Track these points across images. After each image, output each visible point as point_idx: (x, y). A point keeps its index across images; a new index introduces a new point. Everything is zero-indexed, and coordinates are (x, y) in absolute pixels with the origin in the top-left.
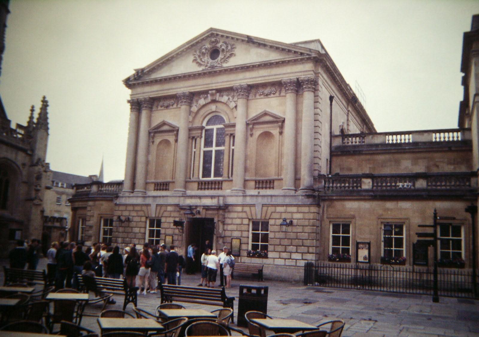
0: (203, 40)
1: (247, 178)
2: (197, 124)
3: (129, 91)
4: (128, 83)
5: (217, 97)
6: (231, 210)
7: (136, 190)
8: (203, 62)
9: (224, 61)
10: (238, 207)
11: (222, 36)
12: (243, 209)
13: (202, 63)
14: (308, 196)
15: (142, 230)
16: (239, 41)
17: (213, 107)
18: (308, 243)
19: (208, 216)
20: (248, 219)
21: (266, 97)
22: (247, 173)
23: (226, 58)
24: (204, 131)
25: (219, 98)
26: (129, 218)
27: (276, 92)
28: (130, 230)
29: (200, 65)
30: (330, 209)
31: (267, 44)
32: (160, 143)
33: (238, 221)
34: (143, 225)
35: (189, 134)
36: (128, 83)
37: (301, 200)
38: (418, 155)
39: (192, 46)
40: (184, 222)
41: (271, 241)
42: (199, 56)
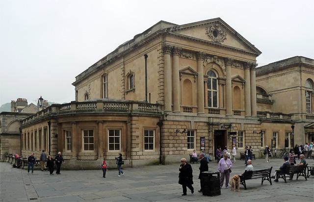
14: (259, 120)
17: (214, 66)
38: (259, 104)
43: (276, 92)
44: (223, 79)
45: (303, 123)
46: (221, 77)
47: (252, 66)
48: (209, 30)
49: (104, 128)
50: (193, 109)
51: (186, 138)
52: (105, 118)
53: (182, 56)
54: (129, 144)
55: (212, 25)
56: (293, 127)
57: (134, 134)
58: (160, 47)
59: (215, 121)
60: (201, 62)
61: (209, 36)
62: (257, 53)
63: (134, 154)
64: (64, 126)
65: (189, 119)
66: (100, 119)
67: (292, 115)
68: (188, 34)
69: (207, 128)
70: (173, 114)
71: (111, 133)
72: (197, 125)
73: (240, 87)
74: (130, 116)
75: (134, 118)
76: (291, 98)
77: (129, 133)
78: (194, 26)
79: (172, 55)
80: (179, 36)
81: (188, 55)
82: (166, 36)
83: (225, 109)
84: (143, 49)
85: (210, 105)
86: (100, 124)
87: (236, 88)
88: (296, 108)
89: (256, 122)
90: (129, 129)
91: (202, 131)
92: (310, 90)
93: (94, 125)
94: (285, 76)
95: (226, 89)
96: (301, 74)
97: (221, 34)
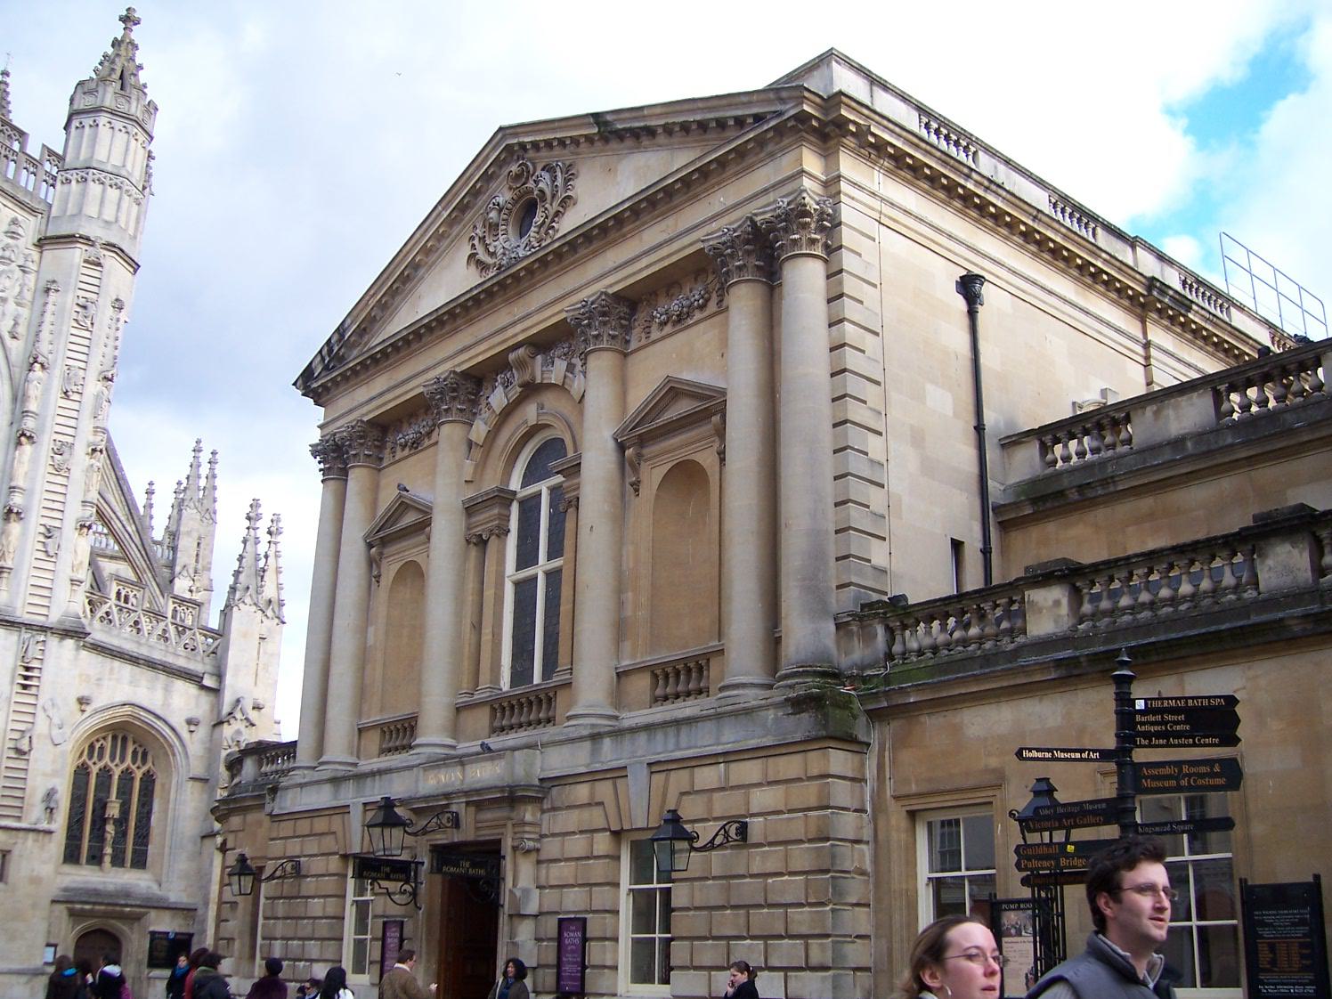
0: (487, 177)
1: (626, 663)
2: (490, 483)
3: (319, 414)
4: (314, 384)
5: (539, 370)
6: (557, 804)
7: (324, 759)
8: (492, 255)
9: (547, 233)
10: (579, 787)
11: (535, 145)
12: (592, 794)
13: (489, 260)
14: (798, 705)
15: (331, 906)
16: (584, 146)
17: (530, 413)
18: (802, 919)
19: (486, 835)
20: (608, 833)
21: (678, 327)
22: (627, 646)
23: (548, 221)
24: (515, 508)
25: (543, 372)
26: (297, 867)
27: (707, 301)
28: (300, 912)
29: (482, 266)
30: (906, 756)
31: (653, 123)
32: (400, 575)
33: (577, 845)
34: (329, 885)
35: (469, 528)
36: (314, 384)
37: (773, 725)
39: (462, 208)
40: (423, 863)
41: (681, 923)
42: (482, 239)
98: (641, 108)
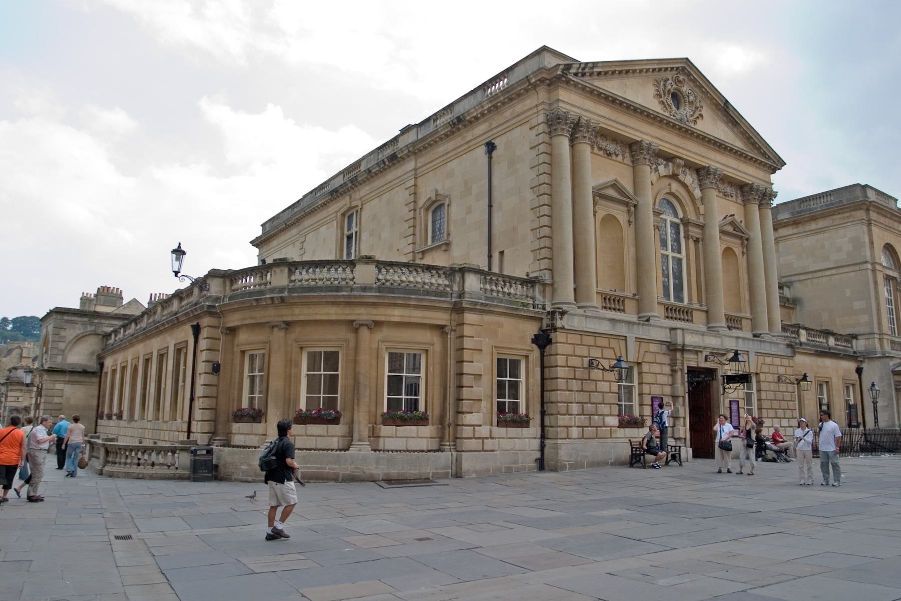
17: (675, 187)
21: (724, 197)
43: (802, 277)
44: (697, 226)
45: (887, 360)
46: (692, 216)
47: (767, 195)
48: (662, 86)
49: (375, 346)
50: (627, 301)
51: (615, 387)
52: (381, 314)
53: (596, 150)
54: (451, 399)
55: (668, 75)
56: (859, 371)
57: (467, 368)
58: (541, 118)
59: (691, 340)
60: (648, 174)
61: (663, 103)
62: (774, 163)
63: (467, 432)
64: (243, 337)
65: (622, 330)
66: (362, 314)
67: (855, 337)
68: (611, 86)
69: (666, 360)
70: (581, 311)
71: (395, 360)
72: (642, 352)
73: (738, 250)
74: (458, 309)
75: (469, 317)
76: (848, 293)
77: (451, 362)
78: (627, 72)
79: (573, 140)
80: (592, 92)
81: (611, 147)
82: (557, 88)
83: (704, 308)
84: (481, 128)
85: (667, 295)
86: (364, 333)
87: (728, 251)
88: (864, 318)
89: (782, 350)
90: (451, 353)
91: (656, 368)
92: (891, 273)
93: (343, 333)
94: (827, 235)
95: (705, 252)
96: (870, 231)
97: (691, 103)
98: (743, 117)
